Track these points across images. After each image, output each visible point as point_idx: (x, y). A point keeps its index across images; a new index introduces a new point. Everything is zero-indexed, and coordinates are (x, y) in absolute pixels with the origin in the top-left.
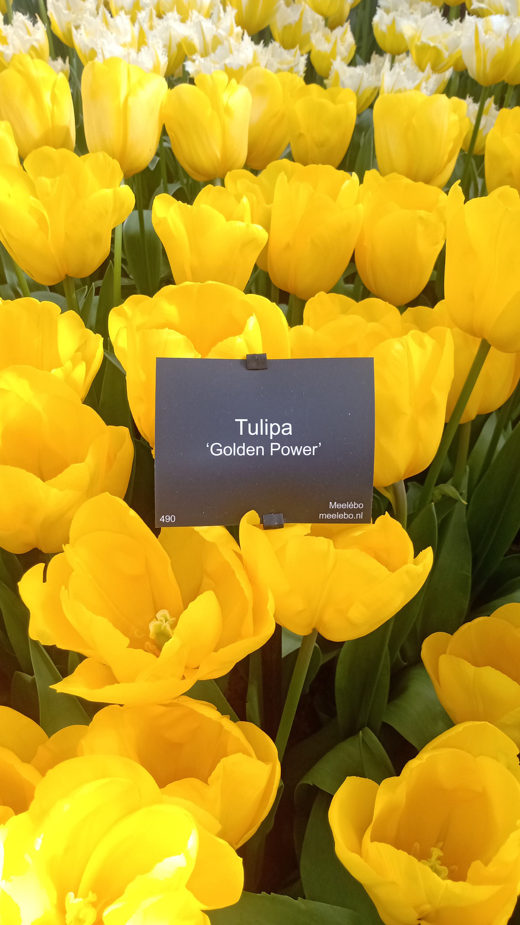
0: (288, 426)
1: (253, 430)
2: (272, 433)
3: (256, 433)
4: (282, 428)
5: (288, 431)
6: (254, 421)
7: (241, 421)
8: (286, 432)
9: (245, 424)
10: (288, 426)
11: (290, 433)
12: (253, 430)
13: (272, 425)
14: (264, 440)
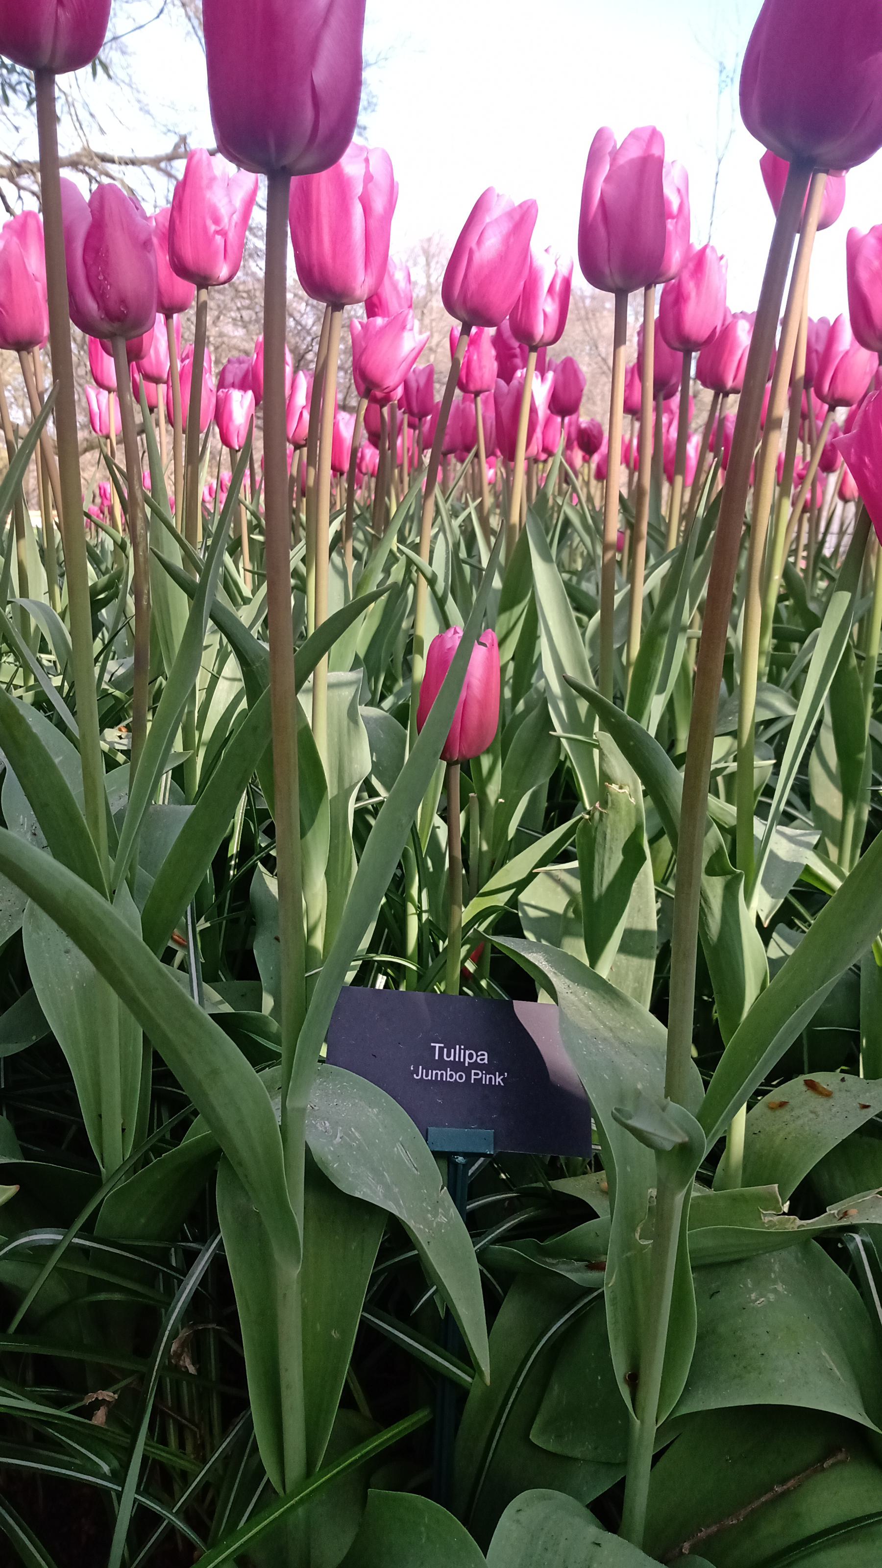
0: (483, 1055)
1: (449, 1056)
2: (467, 1060)
3: (452, 1058)
4: (477, 1056)
5: (482, 1060)
6: (450, 1046)
7: (437, 1045)
8: (481, 1060)
9: (441, 1049)
10: (483, 1055)
11: (486, 1061)
12: (449, 1056)
13: (467, 1052)
14: (457, 1066)
